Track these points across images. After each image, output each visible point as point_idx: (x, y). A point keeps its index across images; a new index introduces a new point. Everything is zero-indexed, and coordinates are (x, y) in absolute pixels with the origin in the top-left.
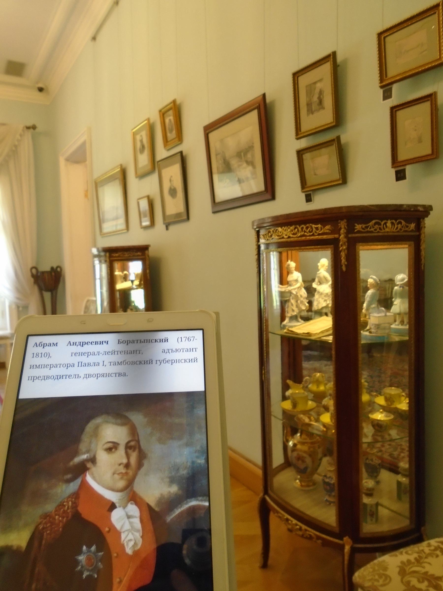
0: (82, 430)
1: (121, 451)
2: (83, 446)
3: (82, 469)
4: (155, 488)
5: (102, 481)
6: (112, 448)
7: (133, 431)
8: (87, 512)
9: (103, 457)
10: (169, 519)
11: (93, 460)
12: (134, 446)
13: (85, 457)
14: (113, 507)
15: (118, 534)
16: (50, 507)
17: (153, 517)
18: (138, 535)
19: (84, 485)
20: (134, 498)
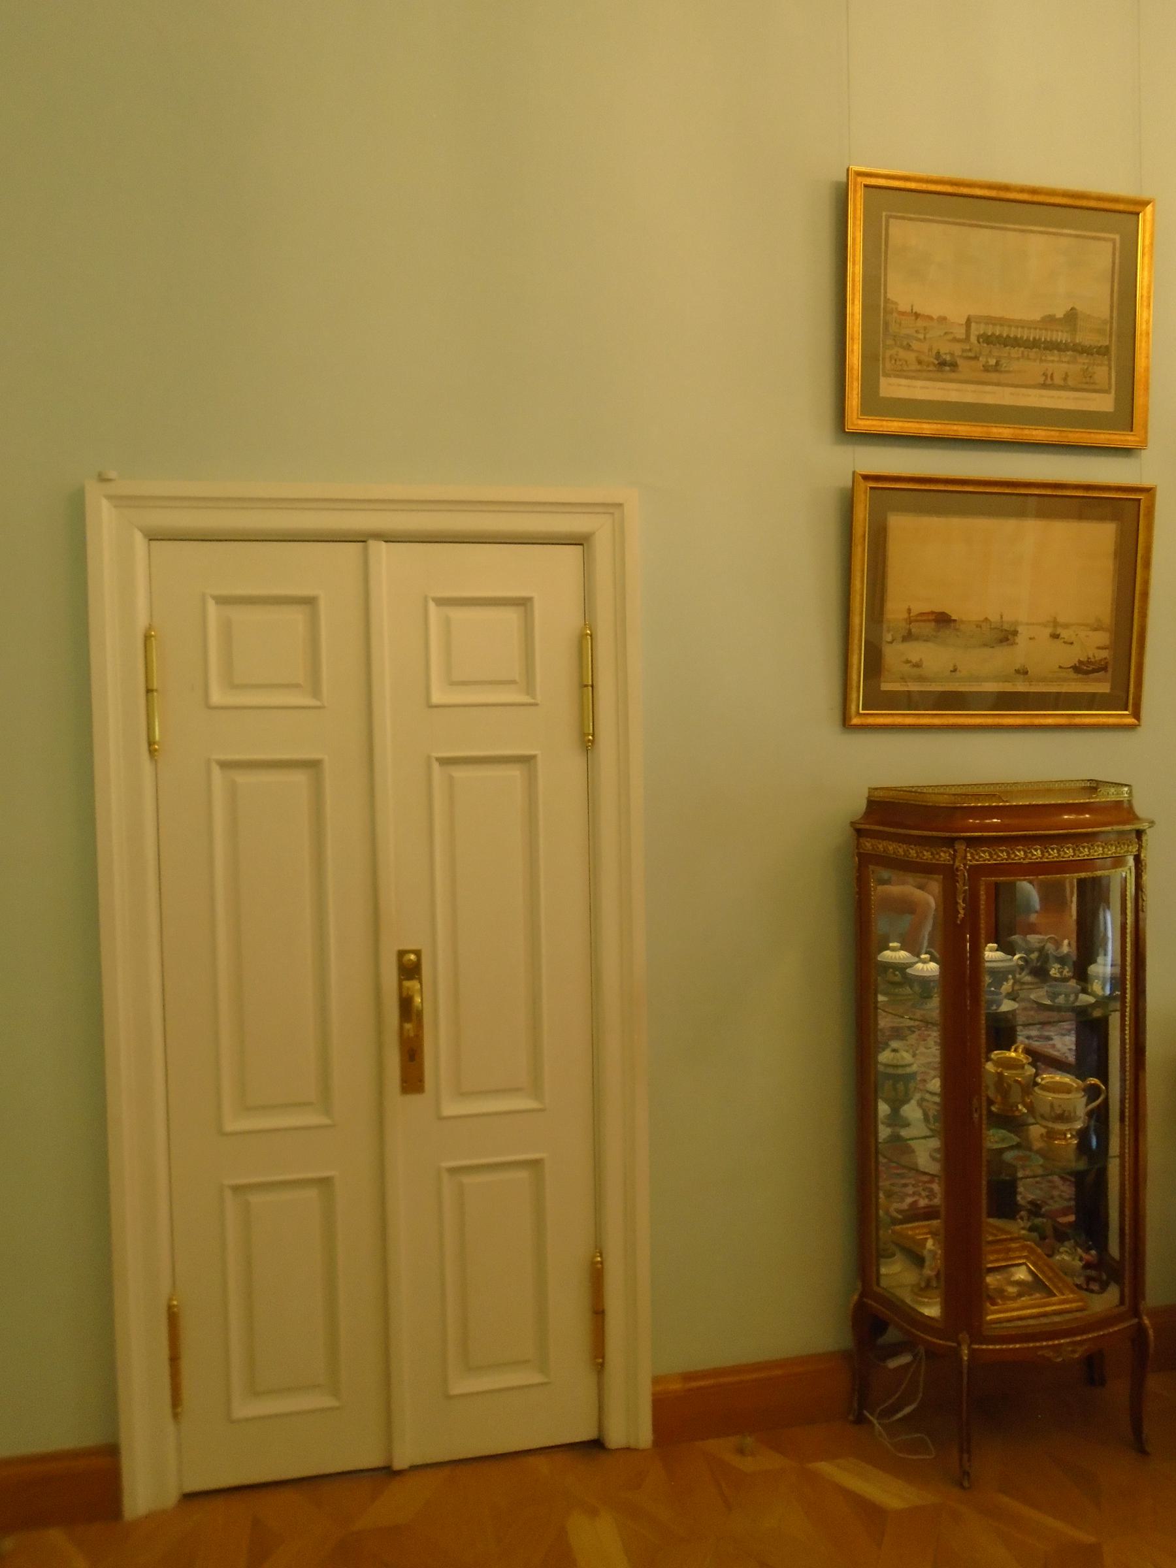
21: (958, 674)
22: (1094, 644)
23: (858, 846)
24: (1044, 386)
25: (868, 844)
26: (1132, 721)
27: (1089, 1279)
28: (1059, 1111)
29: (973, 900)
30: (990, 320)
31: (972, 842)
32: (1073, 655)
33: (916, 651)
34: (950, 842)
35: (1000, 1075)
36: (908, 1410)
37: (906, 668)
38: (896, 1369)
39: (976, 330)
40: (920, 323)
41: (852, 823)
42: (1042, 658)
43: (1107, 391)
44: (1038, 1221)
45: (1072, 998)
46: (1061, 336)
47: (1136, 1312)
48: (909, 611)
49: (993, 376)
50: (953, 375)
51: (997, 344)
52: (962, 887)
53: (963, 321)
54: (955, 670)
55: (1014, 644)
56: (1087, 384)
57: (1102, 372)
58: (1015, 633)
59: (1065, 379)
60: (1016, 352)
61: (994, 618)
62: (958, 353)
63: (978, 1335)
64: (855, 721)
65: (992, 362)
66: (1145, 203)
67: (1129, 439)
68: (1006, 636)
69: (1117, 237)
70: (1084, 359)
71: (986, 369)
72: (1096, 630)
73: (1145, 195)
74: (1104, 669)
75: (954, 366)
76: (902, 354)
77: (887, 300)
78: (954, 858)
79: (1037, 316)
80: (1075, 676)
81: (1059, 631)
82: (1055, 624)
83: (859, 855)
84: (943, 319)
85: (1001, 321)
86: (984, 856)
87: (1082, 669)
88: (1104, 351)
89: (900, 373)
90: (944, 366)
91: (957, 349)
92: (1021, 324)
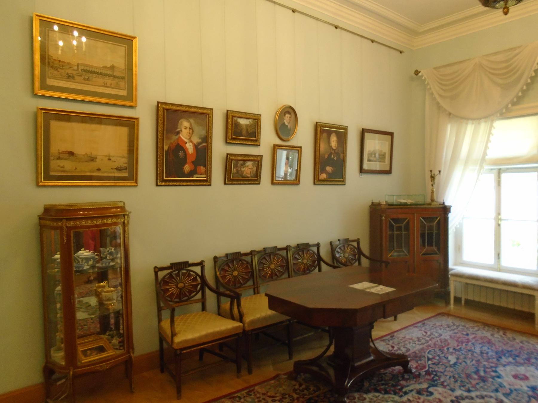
0: (178, 122)
1: (188, 130)
2: (178, 127)
3: (178, 133)
5: (184, 135)
6: (186, 128)
7: (191, 124)
9: (184, 130)
10: (199, 147)
11: (181, 131)
13: (179, 130)
14: (186, 143)
15: (188, 149)
16: (172, 141)
17: (196, 146)
18: (192, 150)
19: (180, 137)
20: (191, 141)
21: (77, 170)
22: (123, 162)
23: (40, 223)
24: (104, 86)
25: (42, 222)
26: (135, 184)
27: (120, 346)
28: (108, 298)
29: (68, 237)
30: (85, 65)
31: (68, 220)
32: (116, 165)
33: (62, 163)
34: (61, 220)
35: (96, 290)
36: (64, 396)
37: (59, 168)
38: (60, 385)
39: (80, 68)
40: (61, 63)
41: (38, 216)
43: (124, 90)
44: (111, 332)
45: (107, 264)
46: (109, 72)
47: (128, 352)
48: (59, 150)
49: (87, 82)
50: (73, 80)
51: (89, 73)
52: (65, 233)
53: (76, 64)
54: (76, 169)
55: (96, 161)
56: (118, 87)
57: (122, 84)
58: (96, 158)
59: (111, 85)
60: (94, 75)
61: (89, 153)
62: (75, 74)
63: (76, 367)
64: (40, 184)
65: (87, 78)
66: (135, 38)
67: (132, 104)
68: (93, 159)
69: (126, 46)
70: (117, 80)
71: (85, 79)
72: (123, 158)
73: (135, 36)
74: (126, 169)
75: (73, 78)
76: (55, 72)
77: (49, 55)
78: (62, 224)
79: (101, 66)
80: (116, 171)
81: (111, 158)
82: (109, 156)
83: (40, 225)
84: (69, 63)
85: (89, 66)
86: (72, 223)
88: (123, 78)
89: (54, 78)
90: (69, 77)
91: (74, 73)
92: (96, 67)
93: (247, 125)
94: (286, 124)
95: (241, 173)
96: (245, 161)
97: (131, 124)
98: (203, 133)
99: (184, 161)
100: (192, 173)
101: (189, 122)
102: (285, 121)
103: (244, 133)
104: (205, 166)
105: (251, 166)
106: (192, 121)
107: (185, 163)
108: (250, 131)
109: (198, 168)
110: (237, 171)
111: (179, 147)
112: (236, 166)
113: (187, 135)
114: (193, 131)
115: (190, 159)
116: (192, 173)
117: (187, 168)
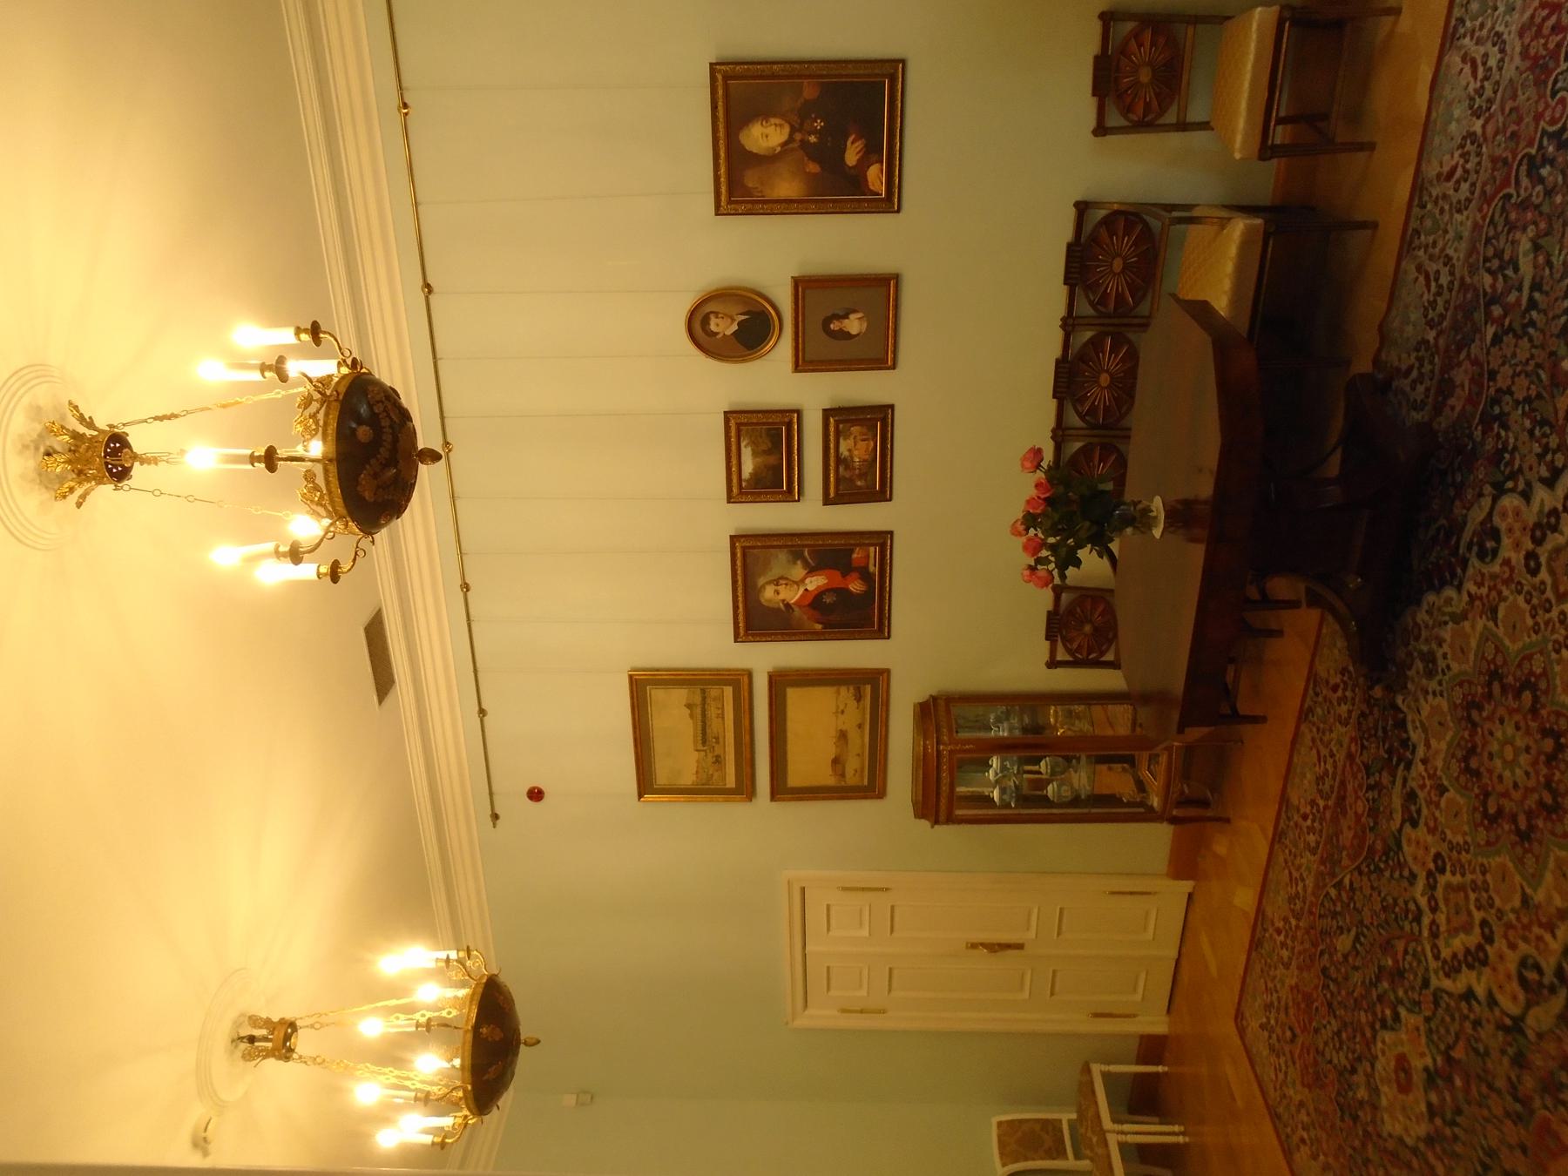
3: (788, 606)
4: (798, 571)
5: (792, 595)
7: (769, 583)
8: (810, 598)
9: (782, 596)
12: (776, 582)
17: (812, 571)
20: (803, 581)
22: (846, 693)
30: (695, 742)
32: (852, 703)
33: (850, 771)
42: (854, 715)
46: (698, 711)
51: (705, 737)
56: (721, 699)
68: (843, 736)
75: (718, 757)
87: (859, 698)
88: (703, 691)
89: (724, 778)
90: (718, 760)
93: (755, 454)
94: (735, 327)
95: (865, 452)
96: (839, 460)
97: (780, 682)
98: (783, 556)
99: (842, 593)
100: (866, 576)
101: (763, 587)
102: (729, 332)
103: (772, 460)
104: (852, 551)
105: (851, 442)
106: (761, 581)
107: (847, 590)
108: (766, 444)
109: (854, 565)
110: (860, 476)
111: (816, 602)
112: (851, 480)
113: (791, 586)
114: (782, 578)
115: (838, 581)
116: (866, 576)
117: (856, 586)
